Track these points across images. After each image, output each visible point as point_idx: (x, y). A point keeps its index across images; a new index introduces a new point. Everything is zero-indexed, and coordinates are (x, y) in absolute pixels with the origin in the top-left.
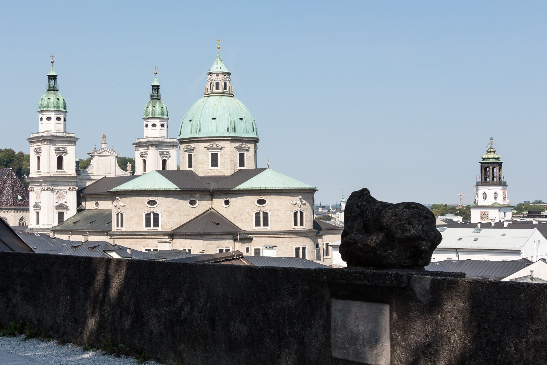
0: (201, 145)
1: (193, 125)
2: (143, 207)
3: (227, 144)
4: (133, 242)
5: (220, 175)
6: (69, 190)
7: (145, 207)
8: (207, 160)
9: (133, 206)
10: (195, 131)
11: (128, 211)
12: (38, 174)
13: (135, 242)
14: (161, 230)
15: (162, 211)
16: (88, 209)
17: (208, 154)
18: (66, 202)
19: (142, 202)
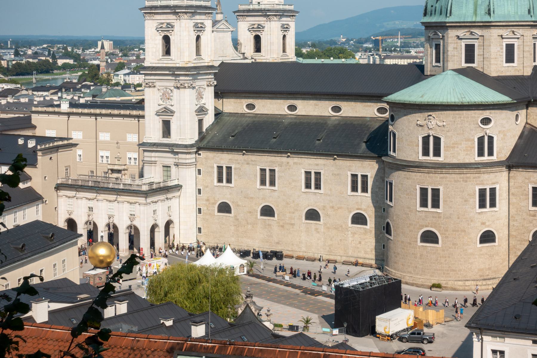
0: (494, 32)
2: (475, 128)
3: (527, 32)
4: (460, 178)
5: (517, 74)
6: (208, 86)
7: (477, 128)
8: (501, 54)
9: (459, 126)
10: (483, 12)
11: (449, 134)
12: (165, 62)
13: (465, 179)
14: (496, 161)
15: (497, 132)
16: (230, 113)
17: (502, 45)
18: (205, 104)
19: (474, 121)
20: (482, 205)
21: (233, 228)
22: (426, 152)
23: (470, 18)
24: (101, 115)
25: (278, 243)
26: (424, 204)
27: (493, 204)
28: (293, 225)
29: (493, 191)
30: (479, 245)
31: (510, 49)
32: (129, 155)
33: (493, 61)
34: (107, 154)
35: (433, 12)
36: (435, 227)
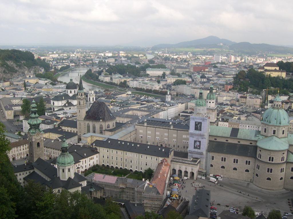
1: (278, 120)
20: (281, 172)
21: (213, 170)
22: (270, 160)
23: (275, 125)
24: (157, 127)
25: (225, 175)
26: (268, 171)
27: (283, 172)
28: (230, 171)
29: (283, 168)
30: (280, 181)
31: (283, 131)
32: (165, 139)
33: (280, 135)
34: (159, 138)
35: (265, 121)
36: (270, 177)
